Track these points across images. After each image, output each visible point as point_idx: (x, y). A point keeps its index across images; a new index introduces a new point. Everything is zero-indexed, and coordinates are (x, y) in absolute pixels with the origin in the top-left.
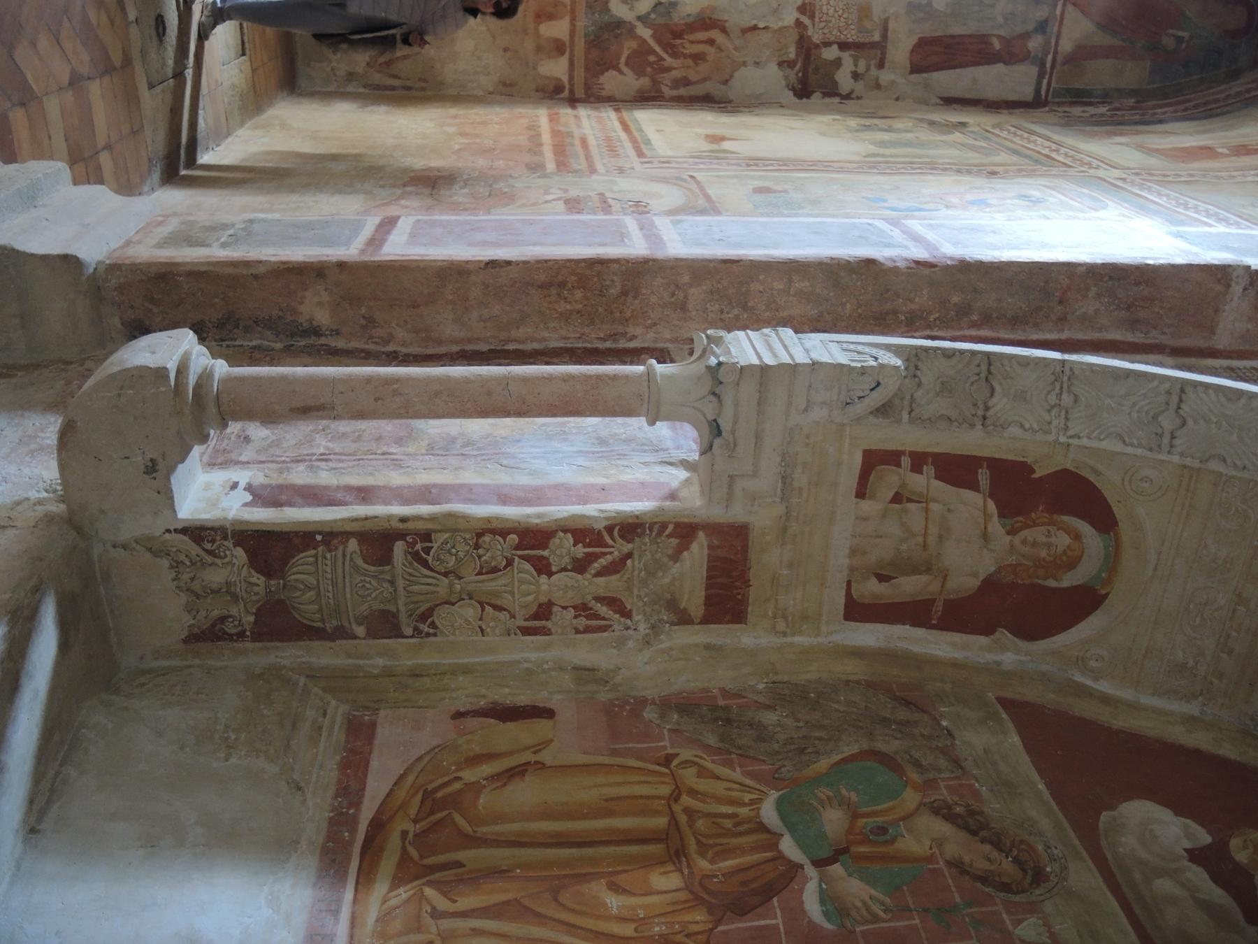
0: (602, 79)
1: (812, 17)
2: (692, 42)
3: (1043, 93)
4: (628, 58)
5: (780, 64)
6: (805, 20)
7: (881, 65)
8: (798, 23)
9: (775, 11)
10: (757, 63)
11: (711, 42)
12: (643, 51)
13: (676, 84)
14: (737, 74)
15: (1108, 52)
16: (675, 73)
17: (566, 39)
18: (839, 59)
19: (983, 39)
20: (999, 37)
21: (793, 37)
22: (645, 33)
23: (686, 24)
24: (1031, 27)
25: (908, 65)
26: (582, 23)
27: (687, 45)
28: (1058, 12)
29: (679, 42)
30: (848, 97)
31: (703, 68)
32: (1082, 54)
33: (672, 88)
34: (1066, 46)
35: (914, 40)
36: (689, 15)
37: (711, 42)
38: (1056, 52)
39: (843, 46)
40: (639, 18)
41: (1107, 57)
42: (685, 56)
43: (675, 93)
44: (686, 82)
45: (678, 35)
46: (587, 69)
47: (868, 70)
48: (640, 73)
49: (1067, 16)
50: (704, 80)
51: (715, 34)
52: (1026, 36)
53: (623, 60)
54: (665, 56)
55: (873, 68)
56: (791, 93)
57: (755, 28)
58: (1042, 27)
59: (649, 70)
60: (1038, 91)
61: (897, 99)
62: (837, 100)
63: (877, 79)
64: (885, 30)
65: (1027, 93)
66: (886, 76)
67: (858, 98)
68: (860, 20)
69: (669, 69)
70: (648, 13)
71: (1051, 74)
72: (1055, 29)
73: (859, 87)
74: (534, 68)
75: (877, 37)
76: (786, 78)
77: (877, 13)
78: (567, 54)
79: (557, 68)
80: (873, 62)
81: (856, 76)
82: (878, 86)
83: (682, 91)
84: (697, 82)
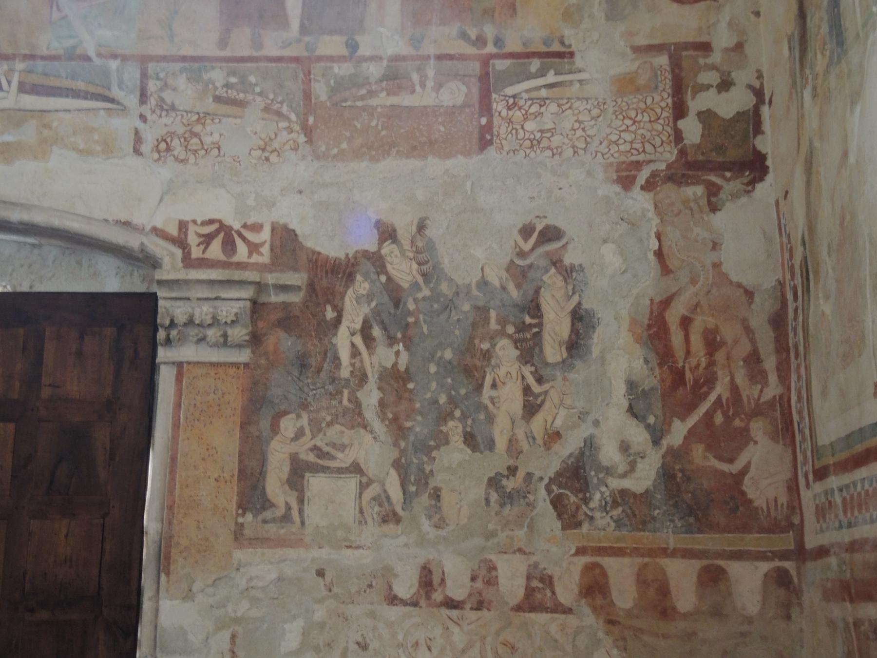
0: (759, 502)
1: (638, 165)
2: (688, 353)
4: (720, 459)
5: (714, 208)
6: (643, 176)
7: (705, 47)
8: (648, 186)
9: (633, 225)
10: (715, 246)
11: (686, 322)
12: (705, 433)
13: (757, 374)
14: (734, 278)
16: (741, 379)
17: (696, 565)
18: (699, 114)
21: (668, 192)
22: (678, 431)
23: (661, 365)
26: (671, 538)
27: (693, 361)
29: (688, 375)
30: (759, 93)
31: (729, 332)
33: (765, 383)
36: (646, 361)
37: (686, 322)
39: (680, 111)
40: (656, 442)
42: (711, 364)
43: (773, 378)
44: (754, 359)
45: (678, 377)
46: (745, 528)
47: (714, 67)
48: (744, 438)
50: (748, 330)
51: (673, 317)
53: (725, 467)
54: (712, 397)
55: (709, 61)
56: (759, 187)
57: (659, 254)
59: (737, 423)
61: (757, 14)
62: (765, 111)
63: (726, 50)
66: (723, 39)
67: (760, 76)
68: (638, 90)
69: (734, 389)
70: (648, 426)
73: (743, 77)
74: (750, 621)
75: (663, 60)
76: (735, 196)
78: (721, 563)
79: (748, 581)
80: (702, 61)
81: (725, 85)
82: (739, 47)
83: (770, 363)
84: (753, 341)
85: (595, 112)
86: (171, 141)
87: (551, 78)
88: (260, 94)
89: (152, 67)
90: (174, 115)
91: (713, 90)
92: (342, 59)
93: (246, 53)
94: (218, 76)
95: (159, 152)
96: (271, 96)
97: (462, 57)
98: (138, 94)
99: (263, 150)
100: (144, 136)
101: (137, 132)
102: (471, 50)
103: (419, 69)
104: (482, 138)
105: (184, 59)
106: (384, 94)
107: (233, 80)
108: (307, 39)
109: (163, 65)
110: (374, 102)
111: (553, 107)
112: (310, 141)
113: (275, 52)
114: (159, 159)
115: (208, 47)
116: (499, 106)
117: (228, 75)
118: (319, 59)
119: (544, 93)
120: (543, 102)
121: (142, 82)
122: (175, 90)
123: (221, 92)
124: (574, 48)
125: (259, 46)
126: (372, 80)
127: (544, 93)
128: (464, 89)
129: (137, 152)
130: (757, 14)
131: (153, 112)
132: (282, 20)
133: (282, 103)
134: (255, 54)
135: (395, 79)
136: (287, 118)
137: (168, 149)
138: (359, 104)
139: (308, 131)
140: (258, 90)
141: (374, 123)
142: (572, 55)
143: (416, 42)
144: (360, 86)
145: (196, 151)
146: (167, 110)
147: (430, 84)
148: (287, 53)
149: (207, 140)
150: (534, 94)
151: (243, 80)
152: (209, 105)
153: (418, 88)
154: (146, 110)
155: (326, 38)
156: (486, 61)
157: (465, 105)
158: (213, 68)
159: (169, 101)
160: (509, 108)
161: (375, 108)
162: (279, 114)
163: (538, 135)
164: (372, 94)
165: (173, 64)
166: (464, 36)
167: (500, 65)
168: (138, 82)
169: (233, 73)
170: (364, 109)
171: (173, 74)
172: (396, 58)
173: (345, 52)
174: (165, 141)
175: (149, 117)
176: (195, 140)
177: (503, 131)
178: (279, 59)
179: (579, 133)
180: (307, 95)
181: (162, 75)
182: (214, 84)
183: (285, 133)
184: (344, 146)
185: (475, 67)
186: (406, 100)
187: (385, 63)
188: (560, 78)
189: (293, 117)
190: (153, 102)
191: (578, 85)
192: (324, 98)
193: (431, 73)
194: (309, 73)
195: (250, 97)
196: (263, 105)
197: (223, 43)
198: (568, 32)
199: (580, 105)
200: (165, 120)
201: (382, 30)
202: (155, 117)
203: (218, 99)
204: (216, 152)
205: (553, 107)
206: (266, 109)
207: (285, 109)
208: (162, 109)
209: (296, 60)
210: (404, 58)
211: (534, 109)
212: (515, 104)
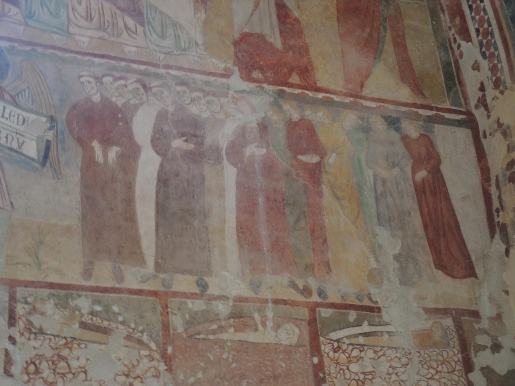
3: (459, 117)
7: (475, 314)
15: (400, 45)
18: (482, 369)
19: (420, 190)
20: (414, 173)
24: (395, 136)
25: (468, 280)
28: (373, 105)
32: (407, 73)
34: (405, 94)
35: (440, 274)
38: (414, 105)
39: (468, 366)
41: (405, 48)
47: (484, 332)
49: (375, 95)
52: (405, 138)
55: (481, 326)
58: (393, 122)
60: (459, 123)
61: (507, 292)
63: (491, 319)
64: (437, 311)
65: (463, 135)
66: (487, 311)
68: (435, 345)
71: (438, 109)
72: (391, 107)
75: (448, 322)
77: (423, 323)
80: (476, 326)
81: (496, 347)
82: (499, 317)
85: (404, 360)
86: (40, 364)
87: (365, 328)
88: (123, 323)
89: (20, 292)
90: (42, 338)
91: (488, 351)
92: (193, 296)
93: (109, 284)
94: (84, 303)
95: (28, 374)
96: (133, 325)
97: (294, 304)
98: (7, 316)
99: (127, 376)
100: (13, 358)
101: (7, 353)
102: (300, 298)
103: (259, 311)
104: (316, 376)
105: (51, 285)
106: (232, 330)
107: (98, 308)
108: (162, 276)
109: (31, 290)
110: (224, 336)
111: (370, 353)
112: (170, 370)
113: (135, 286)
114: (29, 381)
115: (73, 276)
116: (326, 349)
117: (94, 303)
118: (175, 294)
119: (361, 340)
120: (362, 347)
121: (10, 305)
122: (43, 314)
123: (86, 319)
124: (380, 305)
125: (121, 279)
126: (222, 316)
127: (361, 340)
128: (297, 330)
129: (8, 373)
130: (507, 292)
131: (22, 334)
132: (138, 258)
133: (142, 332)
134: (117, 286)
135: (241, 317)
136: (150, 349)
137: (37, 371)
138: (211, 337)
139: (167, 359)
140: (120, 319)
141: (225, 356)
142: (379, 309)
143: (255, 286)
144: (211, 322)
145: (64, 374)
146: (35, 334)
147: (270, 324)
148: (146, 287)
149: (74, 364)
150: (354, 341)
151: (107, 309)
152: (75, 330)
153: (260, 327)
154: (15, 332)
155: (180, 277)
156: (313, 308)
157: (299, 345)
158: (79, 296)
159: (37, 324)
160: (335, 351)
161: (225, 342)
162: (140, 342)
163: (362, 377)
164: (222, 329)
165: (42, 290)
166: (293, 285)
167: (325, 313)
168: (7, 305)
169: (99, 303)
170: (216, 342)
171: (42, 299)
172: (240, 299)
173: (196, 290)
174: (34, 363)
175: (18, 339)
176: (63, 364)
177: (333, 370)
178: (139, 292)
179: (394, 378)
180: (166, 326)
181: (30, 300)
182: (79, 311)
183: (146, 360)
184: (200, 375)
185: (304, 313)
186: (251, 337)
187: (231, 303)
188: (373, 329)
189: (153, 346)
190: (21, 324)
191: (386, 336)
192: (180, 330)
193: (270, 315)
194: (167, 306)
195: (113, 325)
196: (125, 333)
197: (87, 273)
198: (373, 291)
199: (392, 353)
200: (33, 343)
201: (225, 273)
202: (23, 339)
203: (84, 325)
204: (82, 376)
205: (370, 353)
206: (129, 337)
207: (145, 338)
208: (30, 332)
209: (155, 294)
210: (246, 300)
211: (355, 353)
212: (339, 347)
